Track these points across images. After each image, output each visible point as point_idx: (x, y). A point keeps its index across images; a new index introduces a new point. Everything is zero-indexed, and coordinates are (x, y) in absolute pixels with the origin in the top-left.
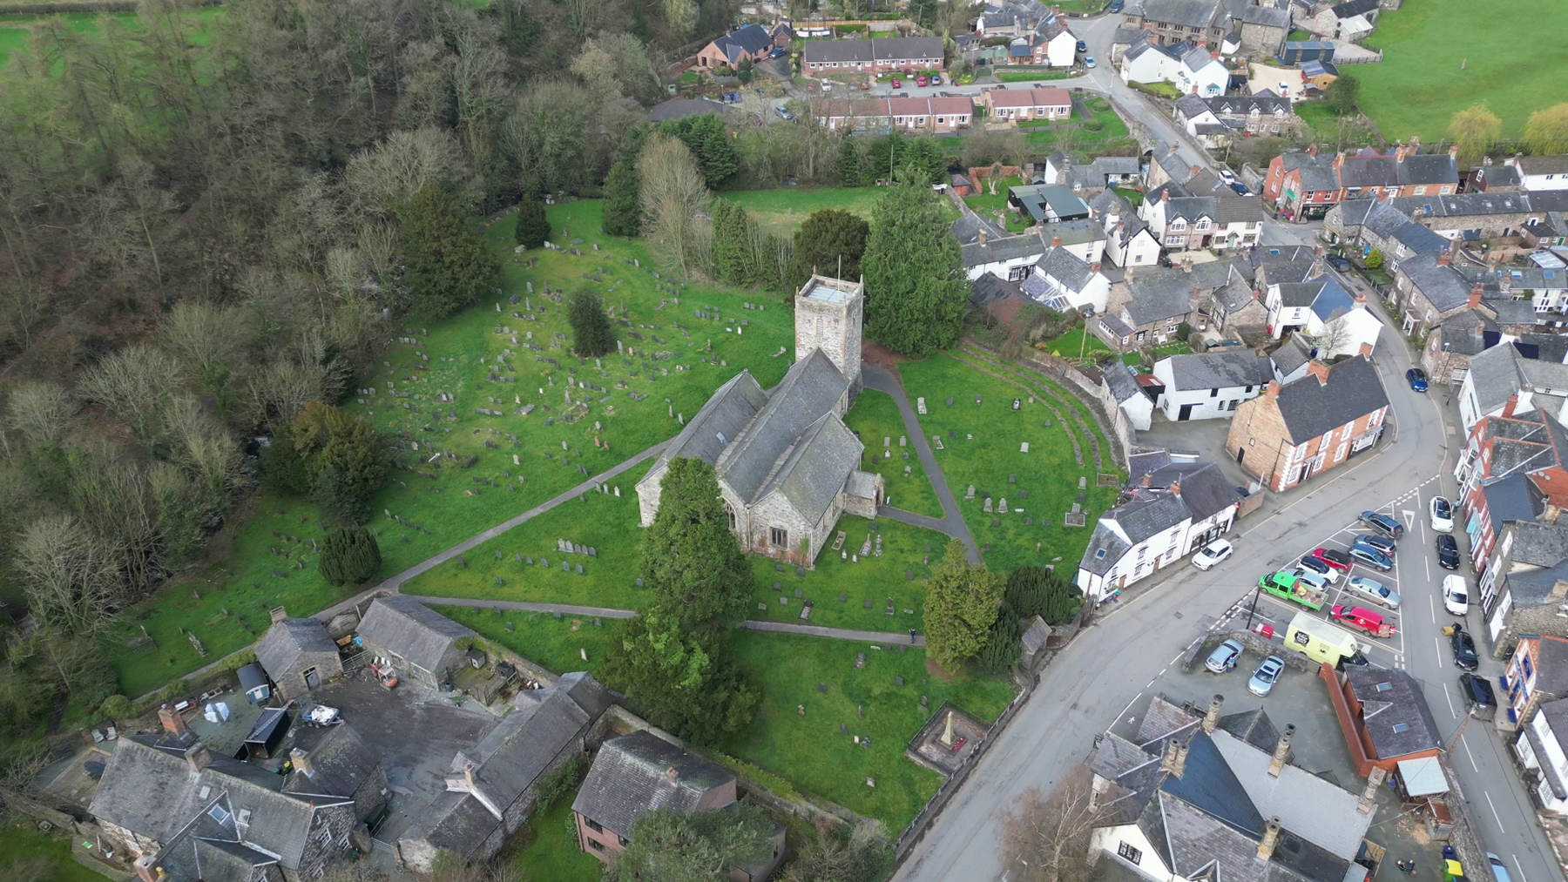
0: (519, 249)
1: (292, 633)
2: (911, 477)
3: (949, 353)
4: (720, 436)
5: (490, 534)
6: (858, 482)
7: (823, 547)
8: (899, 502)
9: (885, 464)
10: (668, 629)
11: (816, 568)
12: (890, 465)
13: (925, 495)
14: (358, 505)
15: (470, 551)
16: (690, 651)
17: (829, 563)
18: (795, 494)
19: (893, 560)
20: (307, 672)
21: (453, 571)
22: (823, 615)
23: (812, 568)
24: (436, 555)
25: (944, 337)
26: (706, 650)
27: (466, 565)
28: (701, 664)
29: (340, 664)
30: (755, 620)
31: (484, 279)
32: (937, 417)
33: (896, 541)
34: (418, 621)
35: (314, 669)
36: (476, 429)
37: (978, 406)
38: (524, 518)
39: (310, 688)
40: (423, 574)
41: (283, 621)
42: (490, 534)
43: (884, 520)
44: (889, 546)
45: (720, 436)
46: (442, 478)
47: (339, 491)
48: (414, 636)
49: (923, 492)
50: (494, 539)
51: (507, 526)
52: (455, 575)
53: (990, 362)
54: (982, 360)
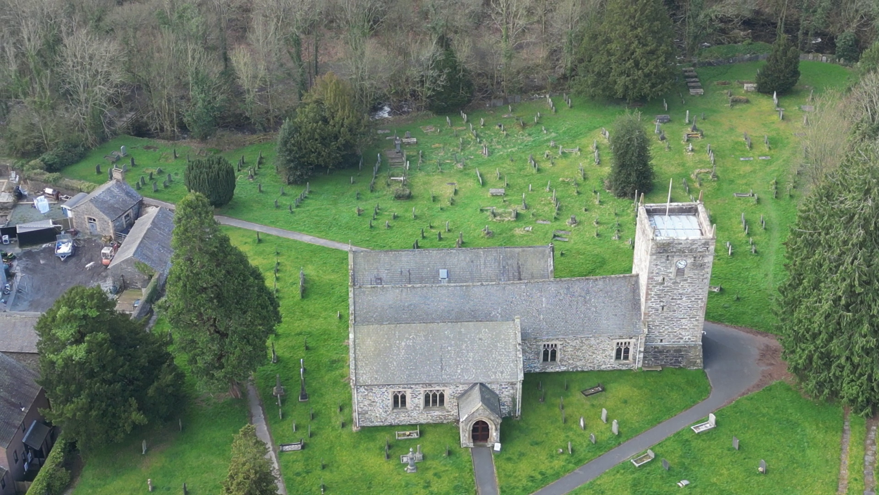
0: (749, 86)
1: (109, 189)
2: (564, 457)
3: (851, 416)
4: (443, 273)
5: (307, 239)
6: (471, 398)
7: (391, 426)
8: (509, 459)
9: (571, 429)
10: (72, 308)
11: (357, 433)
12: (570, 434)
13: (540, 477)
14: (292, 165)
15: (279, 237)
16: (78, 341)
17: (373, 439)
18: (369, 342)
19: (407, 485)
20: (91, 219)
21: (249, 240)
22: (296, 461)
23: (354, 429)
24: (266, 225)
25: (848, 390)
26: (89, 352)
27: (260, 241)
28: (72, 356)
29: (112, 231)
30: (265, 419)
31: (635, 82)
32: (696, 444)
33: (440, 477)
34: (146, 234)
35: (94, 220)
36: (455, 182)
37: (751, 472)
38: (337, 245)
39: (91, 233)
40: (240, 228)
41: (118, 181)
42: (307, 239)
43: (466, 457)
44: (429, 475)
45: (443, 273)
46: (377, 194)
47: (285, 143)
48: (134, 241)
49: (542, 474)
50: (300, 243)
51: (322, 242)
52: (246, 243)
53: (870, 458)
54: (865, 449)
